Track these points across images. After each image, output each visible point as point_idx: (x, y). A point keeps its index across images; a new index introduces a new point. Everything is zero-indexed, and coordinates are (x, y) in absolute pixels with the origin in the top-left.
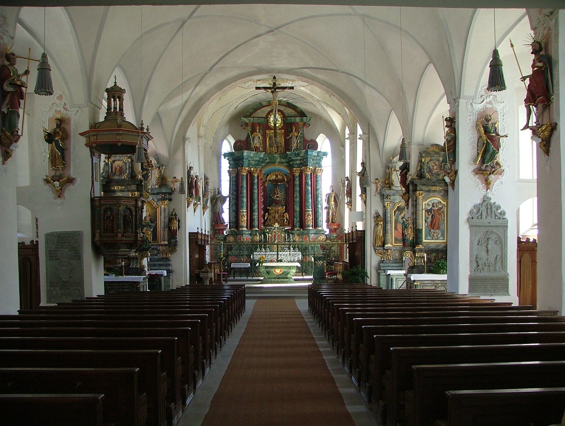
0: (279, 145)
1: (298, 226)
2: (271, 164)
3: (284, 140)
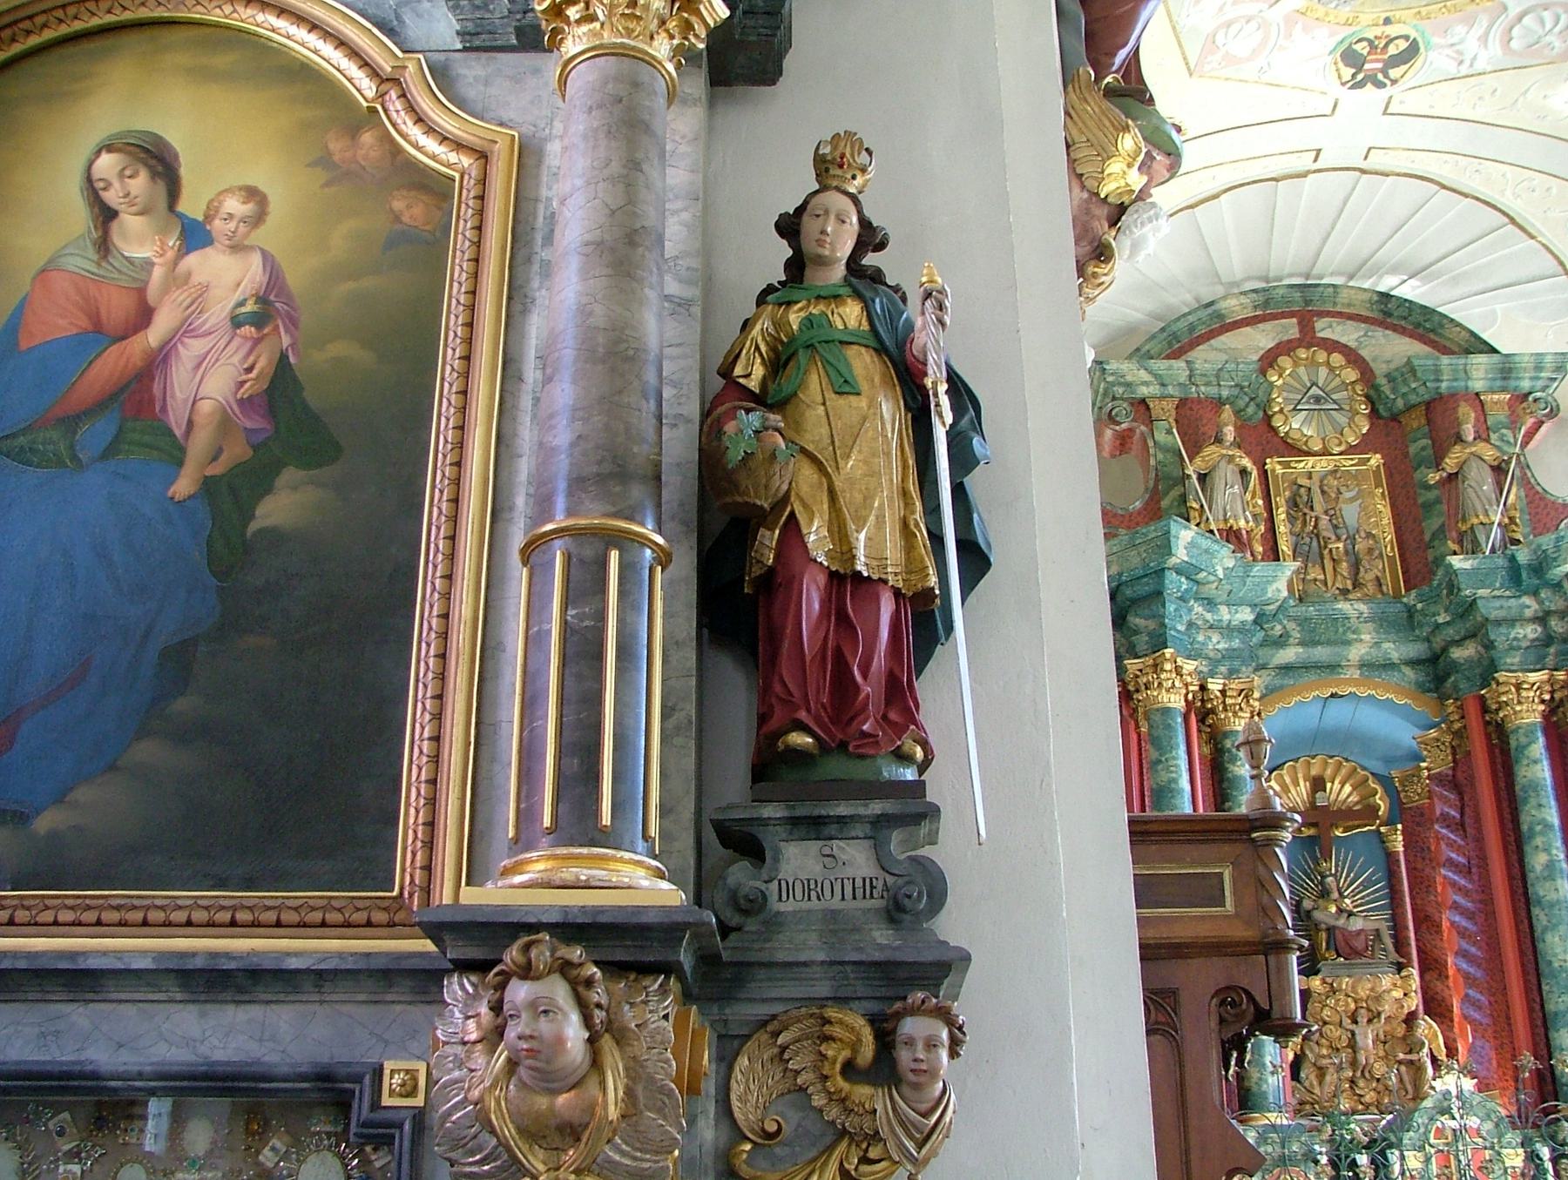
0: (1361, 546)
2: (1312, 677)
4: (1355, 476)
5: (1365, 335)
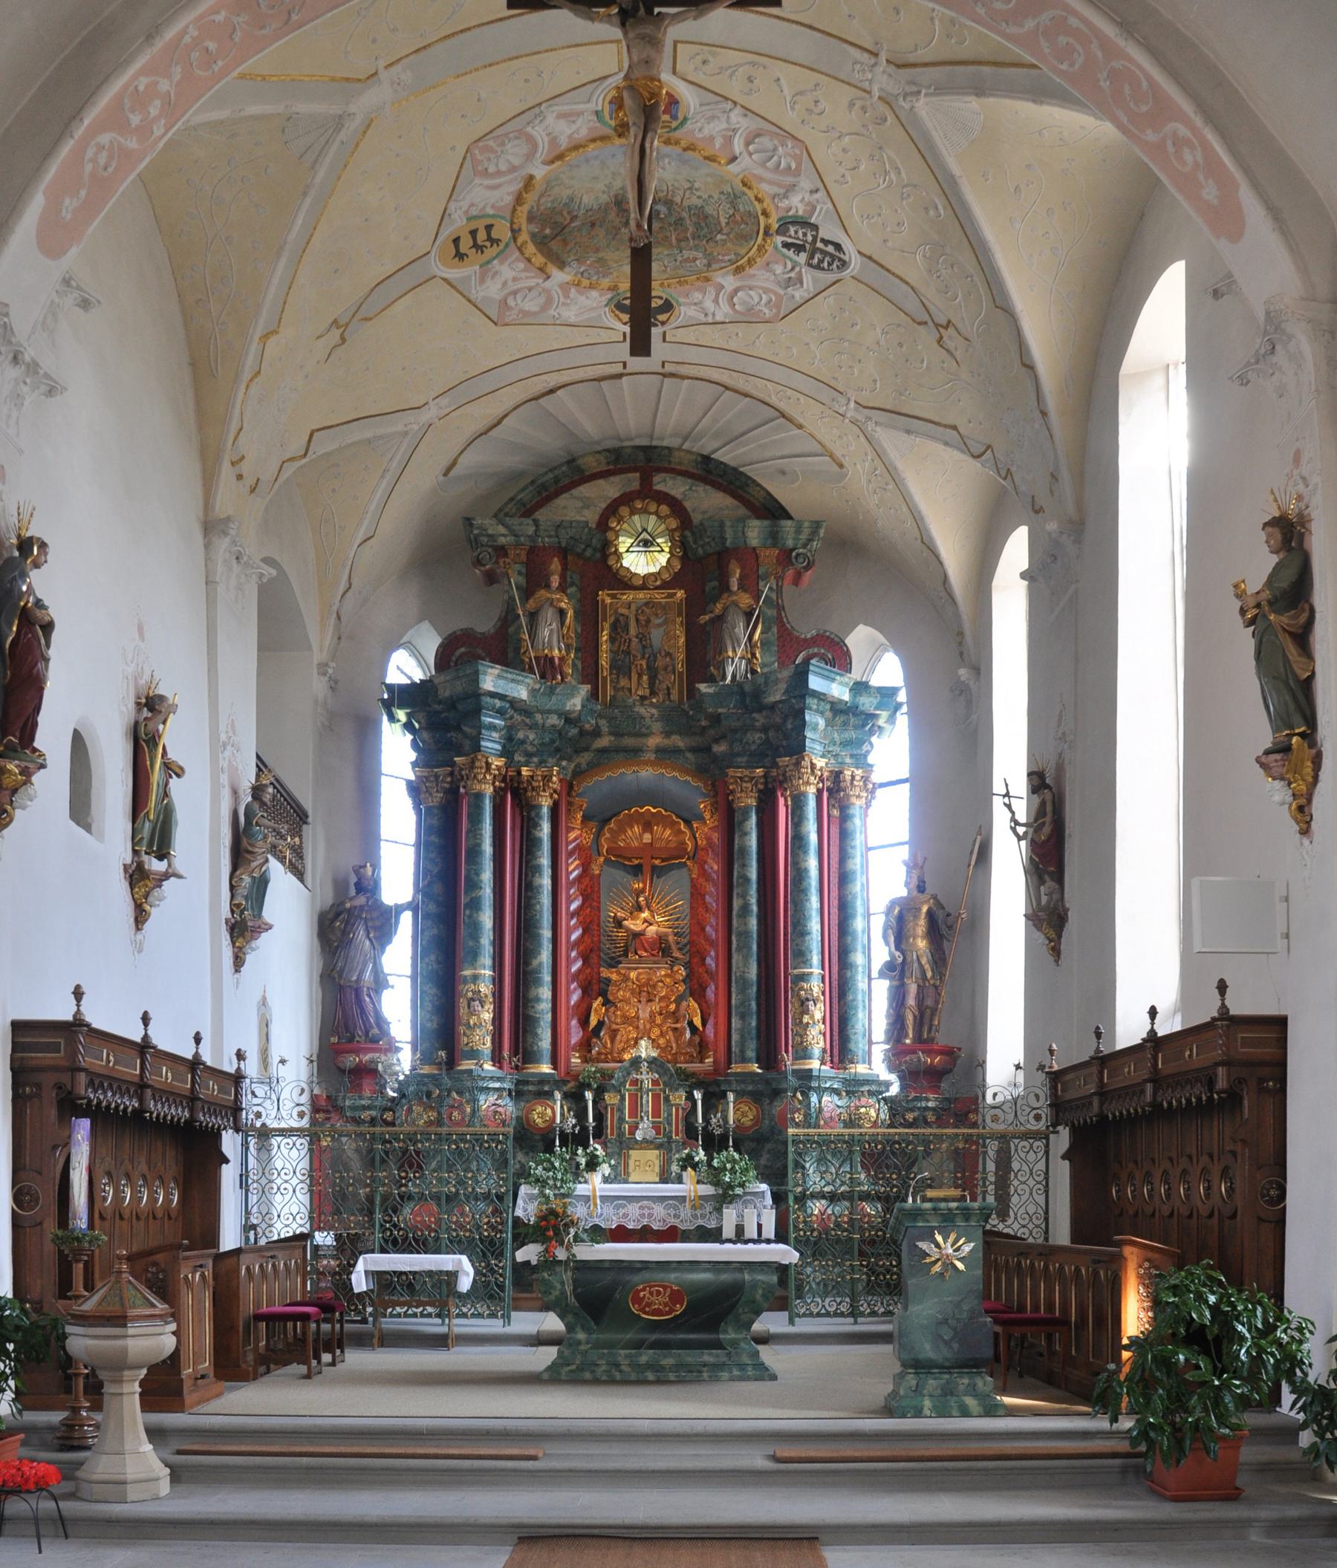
0: (660, 663)
1: (751, 1054)
3: (682, 640)
4: (664, 607)
5: (690, 489)
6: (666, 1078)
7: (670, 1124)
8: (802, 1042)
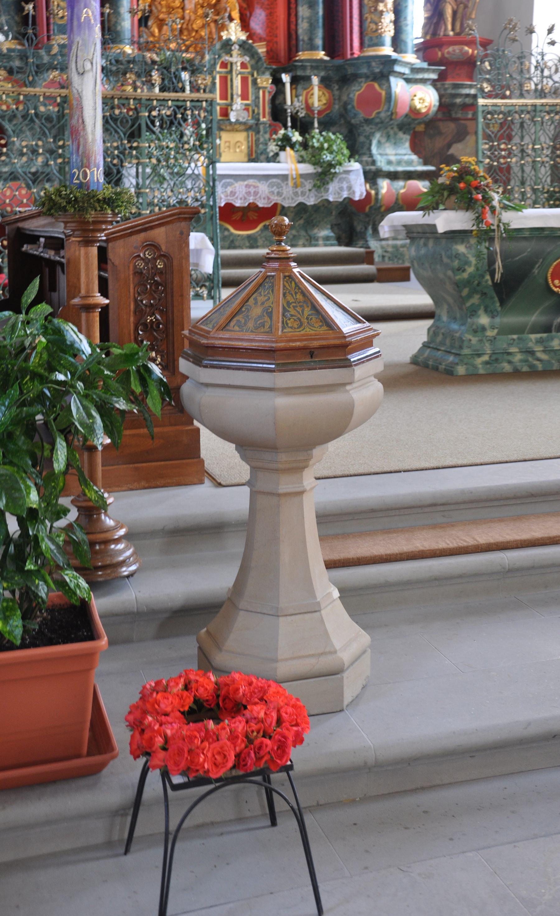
6: (253, 62)
7: (257, 106)
8: (377, 30)
